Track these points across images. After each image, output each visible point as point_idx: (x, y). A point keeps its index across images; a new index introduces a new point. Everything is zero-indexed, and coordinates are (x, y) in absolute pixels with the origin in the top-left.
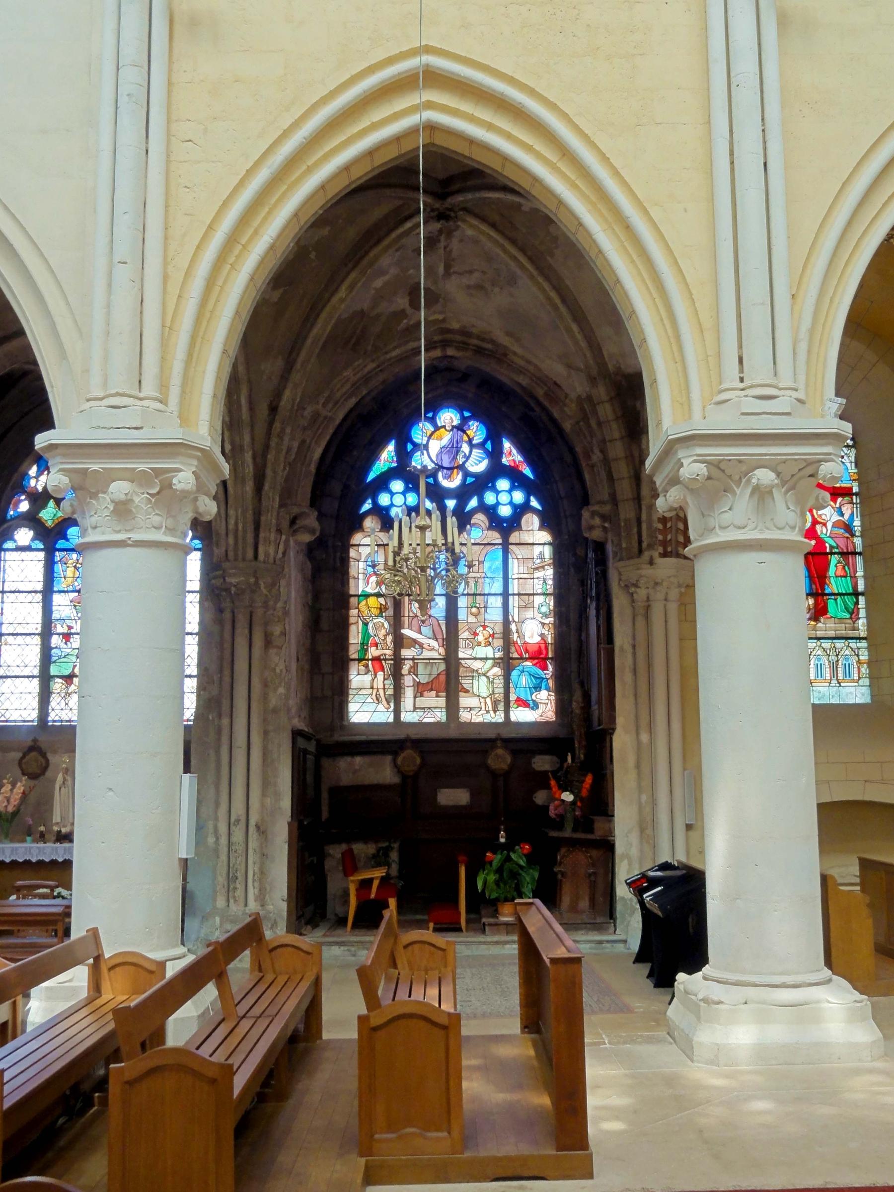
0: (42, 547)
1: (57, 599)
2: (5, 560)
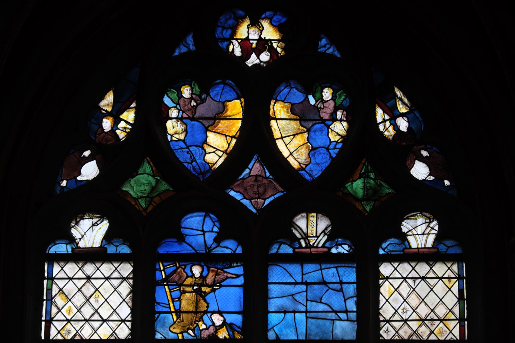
2: (51, 279)
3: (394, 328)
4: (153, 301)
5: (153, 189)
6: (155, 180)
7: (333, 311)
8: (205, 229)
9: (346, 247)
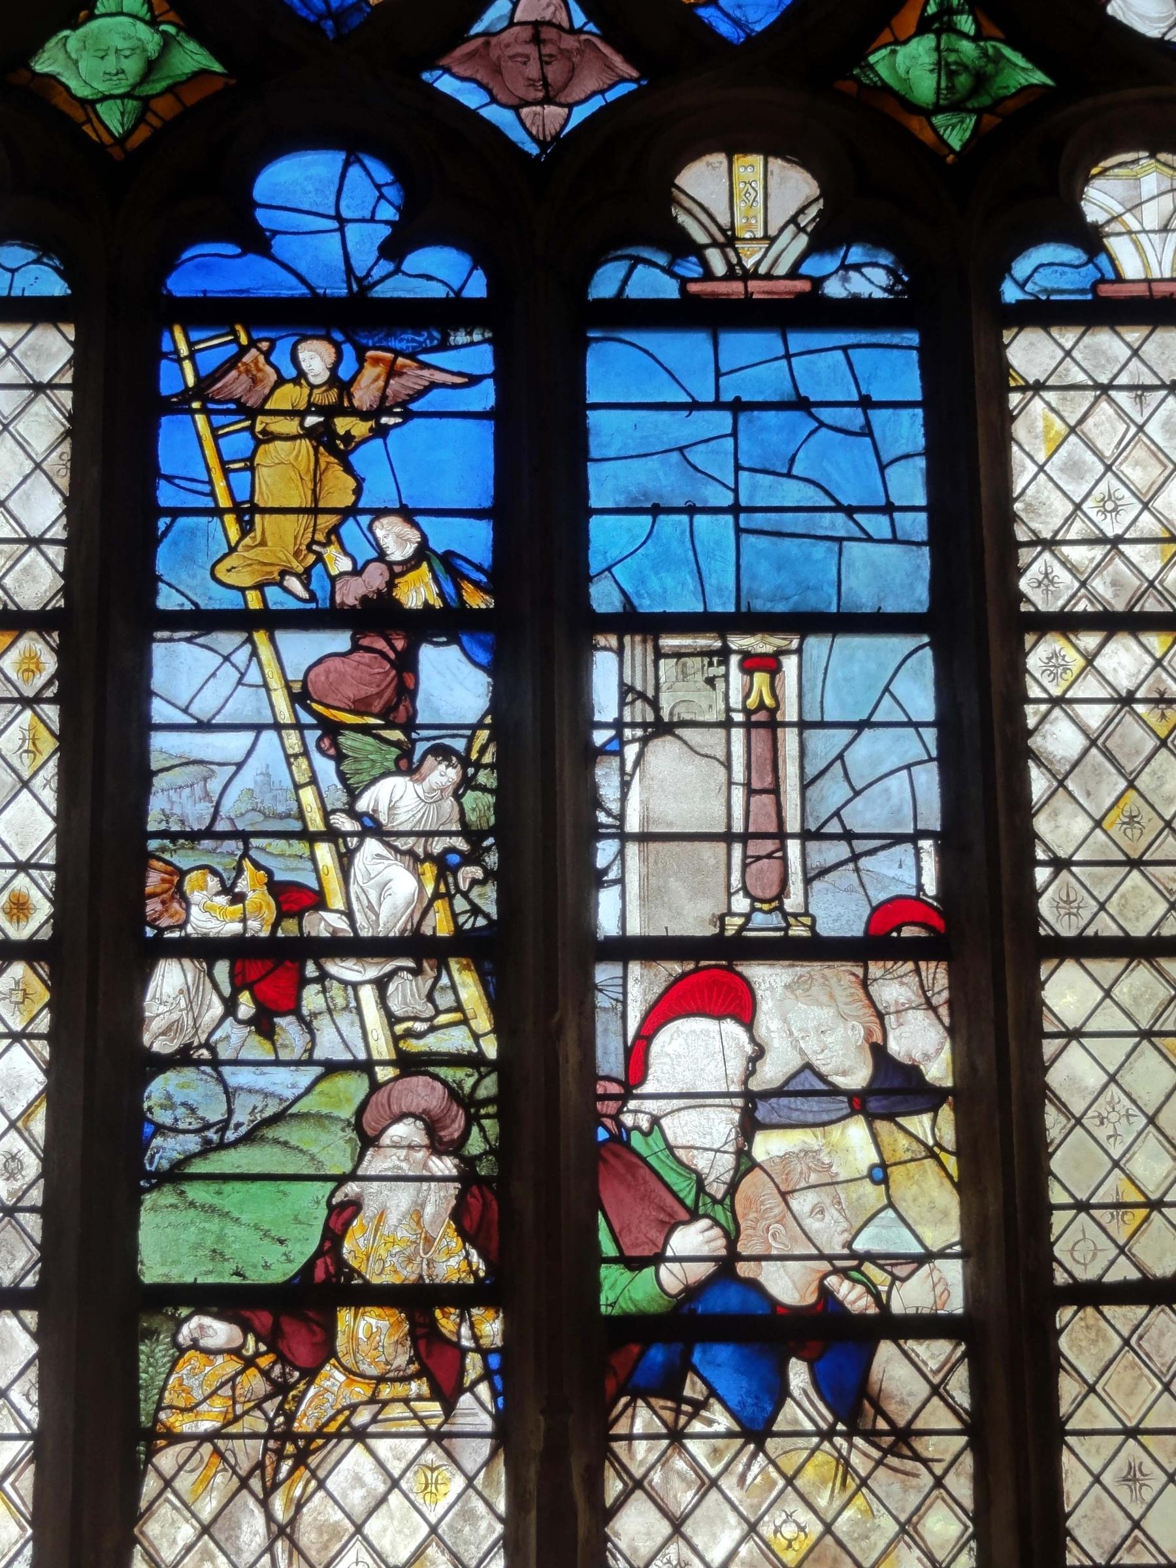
0: (57, 287)
1: (182, 672)
3: (1072, 569)
4: (147, 471)
5: (151, 67)
6: (157, 37)
7: (838, 508)
8: (346, 213)
9: (880, 277)
